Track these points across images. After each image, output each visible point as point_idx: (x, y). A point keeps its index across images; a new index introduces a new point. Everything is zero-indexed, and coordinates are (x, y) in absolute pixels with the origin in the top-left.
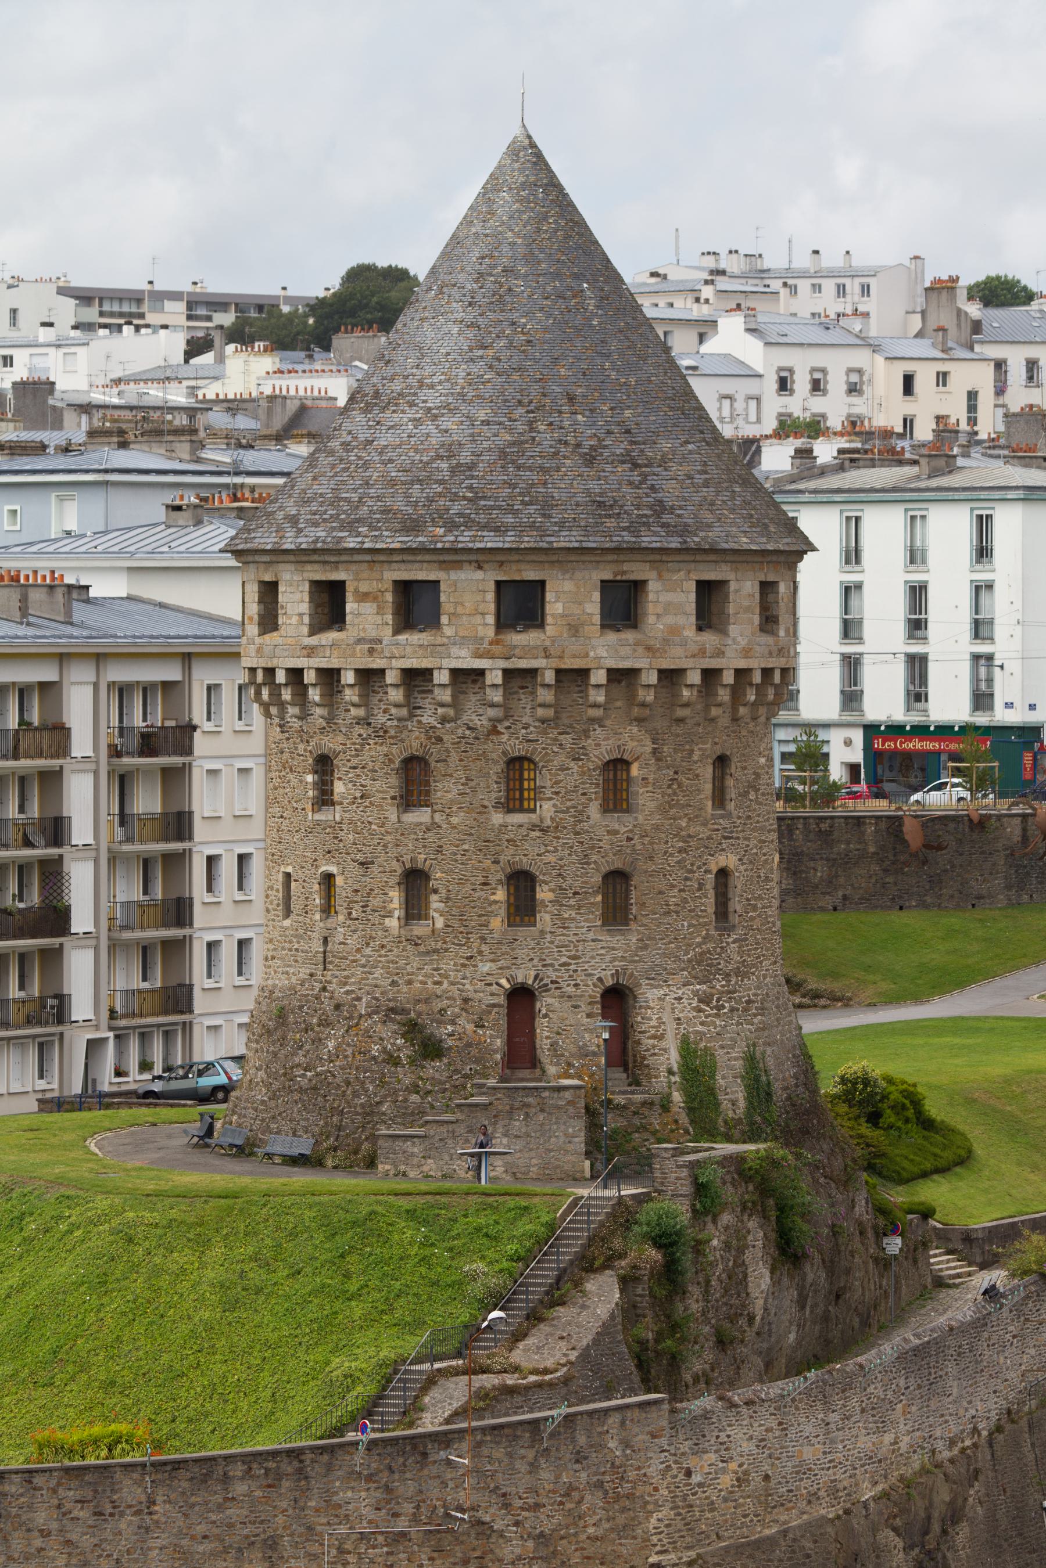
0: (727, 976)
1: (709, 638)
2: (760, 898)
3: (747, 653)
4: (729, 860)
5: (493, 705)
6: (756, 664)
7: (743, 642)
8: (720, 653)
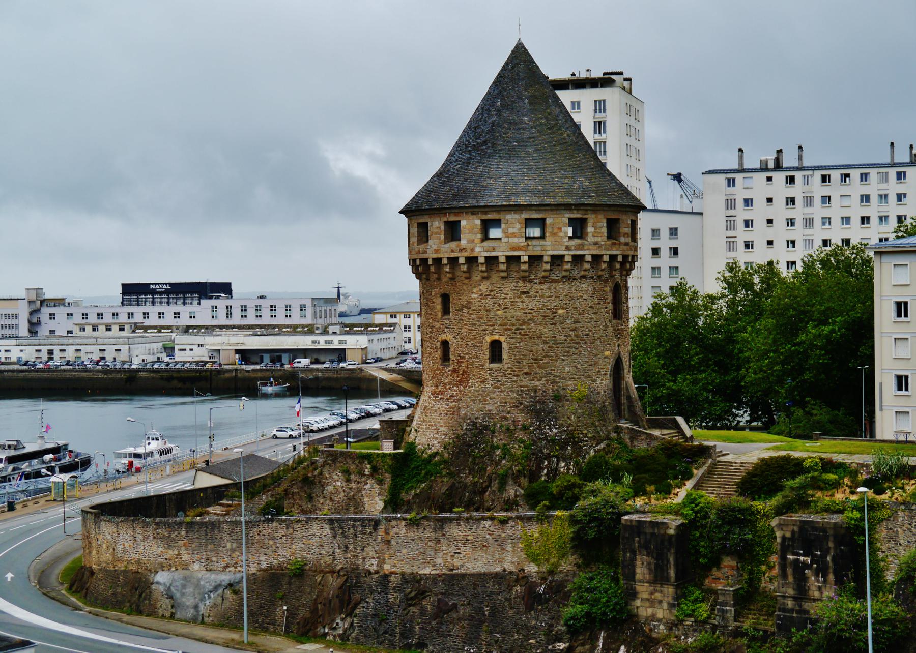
0: (445, 385)
1: (422, 247)
2: (467, 354)
3: (437, 251)
4: (449, 337)
5: (502, 271)
6: (444, 255)
7: (435, 247)
8: (425, 252)
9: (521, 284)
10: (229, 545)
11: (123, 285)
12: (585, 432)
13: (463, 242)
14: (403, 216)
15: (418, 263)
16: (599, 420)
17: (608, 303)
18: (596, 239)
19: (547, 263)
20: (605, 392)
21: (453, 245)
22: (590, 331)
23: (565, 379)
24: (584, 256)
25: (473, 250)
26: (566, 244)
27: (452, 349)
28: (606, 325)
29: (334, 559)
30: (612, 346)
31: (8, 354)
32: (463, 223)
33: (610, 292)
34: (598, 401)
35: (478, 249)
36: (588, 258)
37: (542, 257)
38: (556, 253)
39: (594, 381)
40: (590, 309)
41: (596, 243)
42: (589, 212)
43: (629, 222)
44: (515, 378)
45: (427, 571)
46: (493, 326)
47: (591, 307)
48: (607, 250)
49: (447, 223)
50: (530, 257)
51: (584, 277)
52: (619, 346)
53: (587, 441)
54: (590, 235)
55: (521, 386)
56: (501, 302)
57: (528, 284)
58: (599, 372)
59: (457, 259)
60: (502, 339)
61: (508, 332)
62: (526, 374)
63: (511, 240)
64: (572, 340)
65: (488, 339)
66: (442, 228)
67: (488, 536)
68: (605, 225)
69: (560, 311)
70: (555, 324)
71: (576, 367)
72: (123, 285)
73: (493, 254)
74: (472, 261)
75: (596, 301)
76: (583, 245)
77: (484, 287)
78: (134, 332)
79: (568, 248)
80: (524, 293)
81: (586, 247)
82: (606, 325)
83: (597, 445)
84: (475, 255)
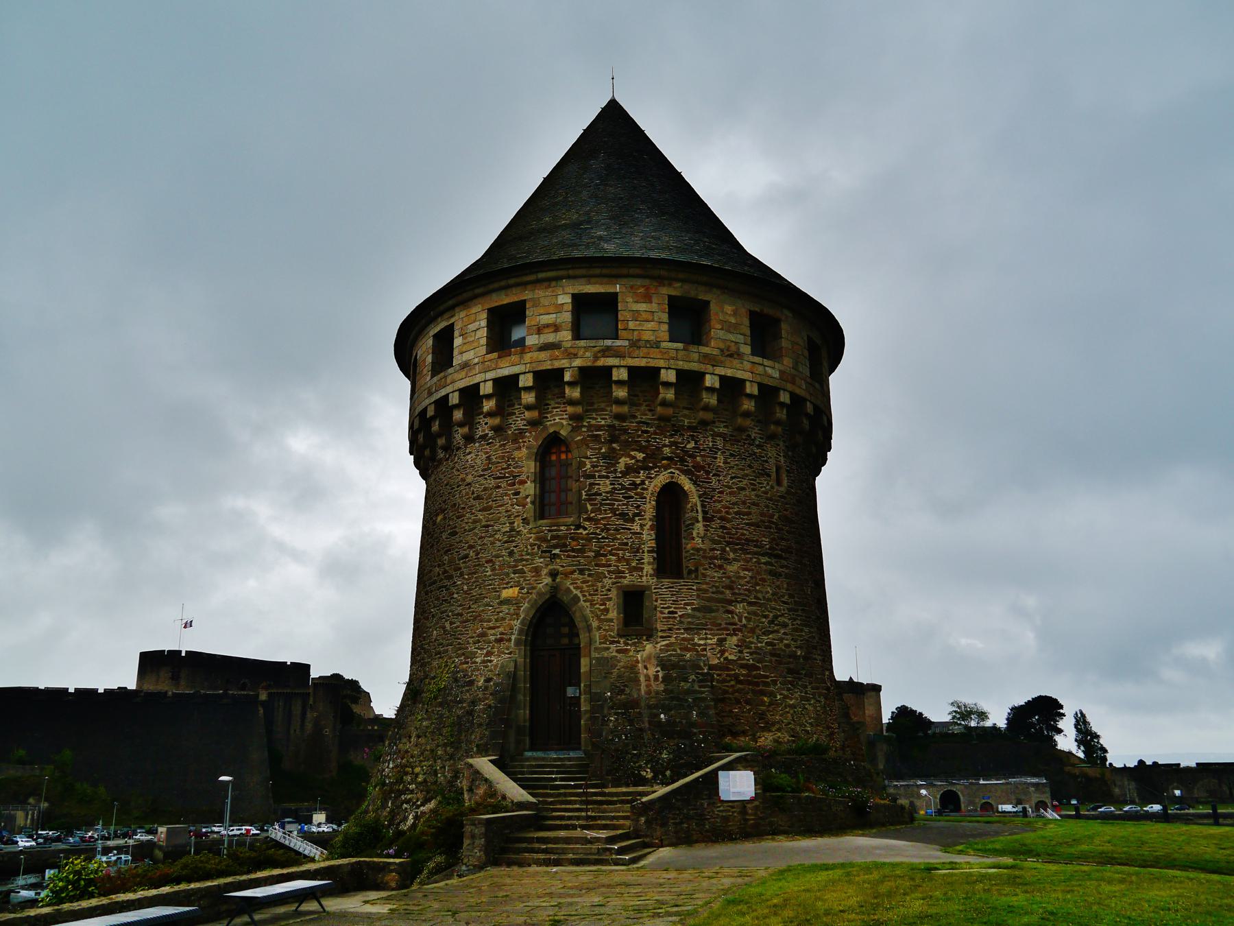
12: (417, 770)
16: (445, 745)
17: (523, 482)
18: (466, 357)
20: (488, 680)
22: (471, 547)
28: (512, 530)
30: (529, 575)
33: (528, 458)
34: (461, 702)
40: (476, 503)
42: (457, 309)
43: (565, 299)
47: (478, 498)
51: (469, 439)
52: (553, 574)
53: (412, 792)
58: (483, 635)
64: (445, 572)
68: (484, 323)
71: (444, 628)
75: (493, 482)
76: (445, 377)
81: (449, 381)
82: (512, 530)
83: (423, 804)
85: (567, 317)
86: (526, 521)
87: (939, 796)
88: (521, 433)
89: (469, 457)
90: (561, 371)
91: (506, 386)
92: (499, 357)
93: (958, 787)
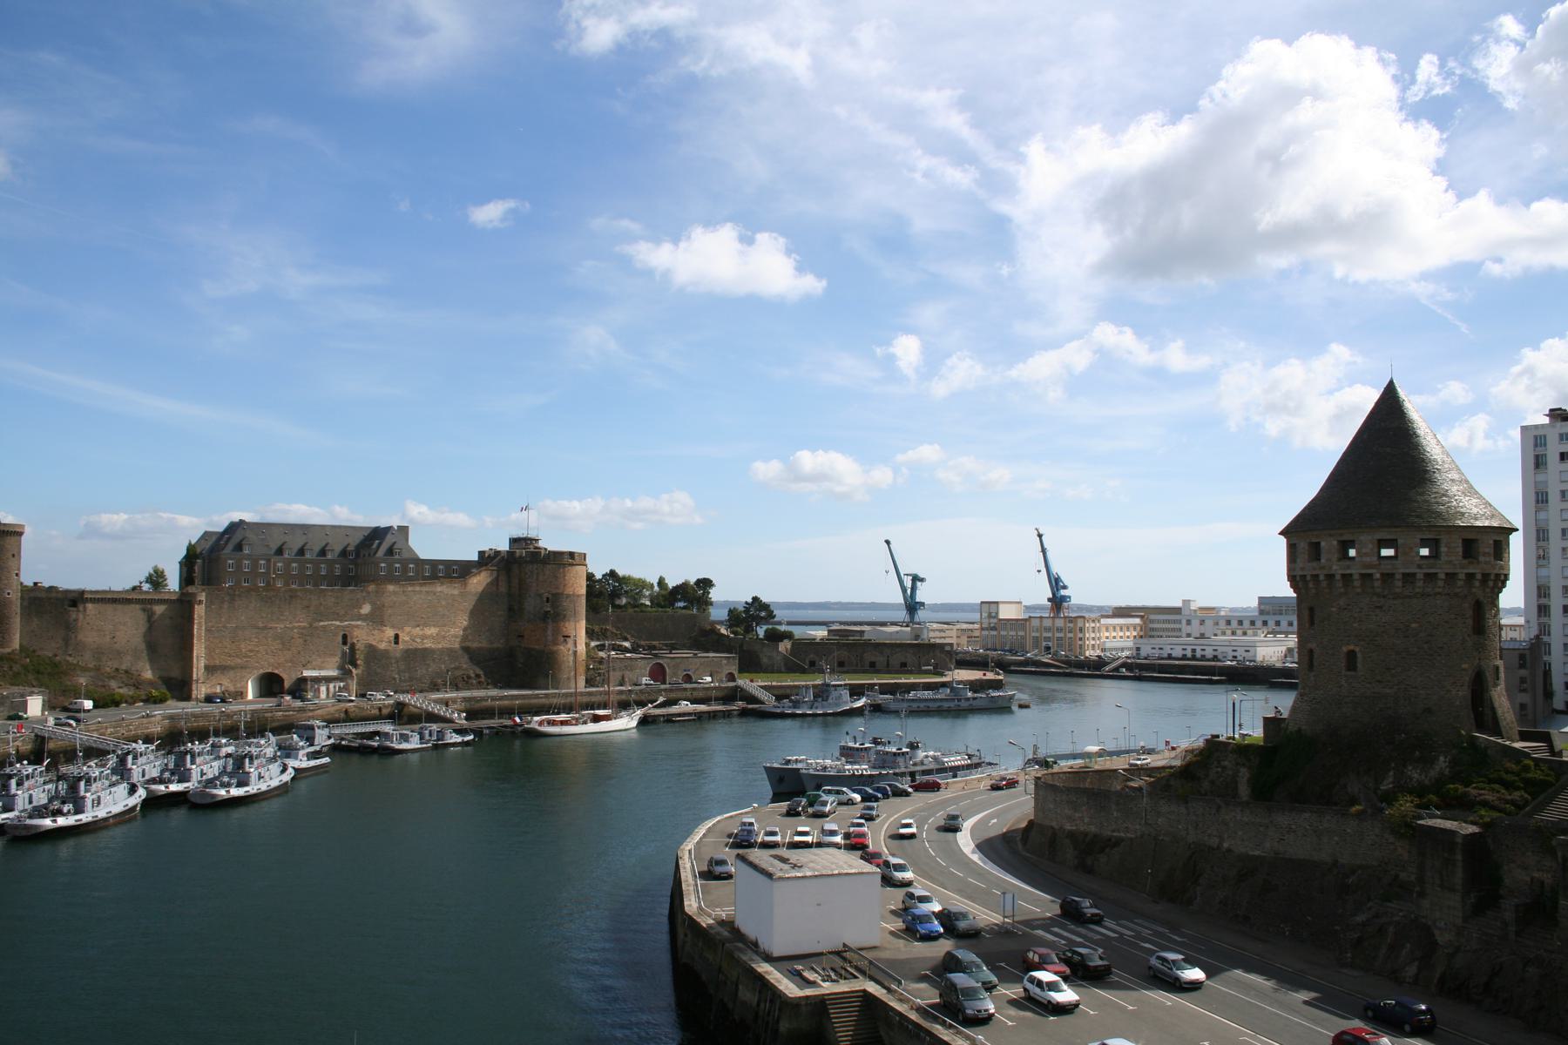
3: (1302, 569)
6: (1308, 573)
7: (1301, 565)
9: (1375, 599)
10: (1115, 814)
11: (1260, 598)
13: (1323, 561)
14: (1282, 537)
15: (1298, 578)
17: (1466, 618)
19: (1399, 580)
21: (1315, 564)
23: (1416, 687)
24: (1436, 573)
25: (1331, 568)
26: (1418, 562)
27: (1315, 656)
29: (1188, 834)
31: (1161, 652)
32: (1323, 544)
35: (1335, 567)
36: (1442, 576)
37: (1393, 574)
38: (1407, 571)
39: (1449, 691)
41: (1450, 562)
43: (1491, 542)
44: (1368, 685)
45: (1257, 853)
46: (1349, 636)
47: (1446, 622)
48: (1463, 568)
49: (1311, 544)
50: (1382, 574)
52: (1479, 659)
54: (1443, 554)
55: (1374, 693)
56: (1356, 615)
57: (1382, 599)
59: (1317, 576)
60: (1357, 649)
61: (1362, 643)
62: (1379, 681)
63: (1364, 559)
65: (1345, 649)
66: (1307, 548)
67: (1308, 827)
68: (1460, 545)
69: (1413, 625)
70: (1408, 637)
72: (1260, 598)
73: (1348, 572)
74: (1330, 577)
75: (1453, 616)
77: (1342, 602)
78: (1265, 636)
79: (1419, 567)
80: (1380, 607)
84: (1332, 572)
85: (1492, 551)
86: (1469, 635)
87: (648, 669)
88: (1466, 596)
89: (1438, 602)
90: (1489, 575)
91: (1470, 576)
92: (1469, 563)
93: (665, 660)
